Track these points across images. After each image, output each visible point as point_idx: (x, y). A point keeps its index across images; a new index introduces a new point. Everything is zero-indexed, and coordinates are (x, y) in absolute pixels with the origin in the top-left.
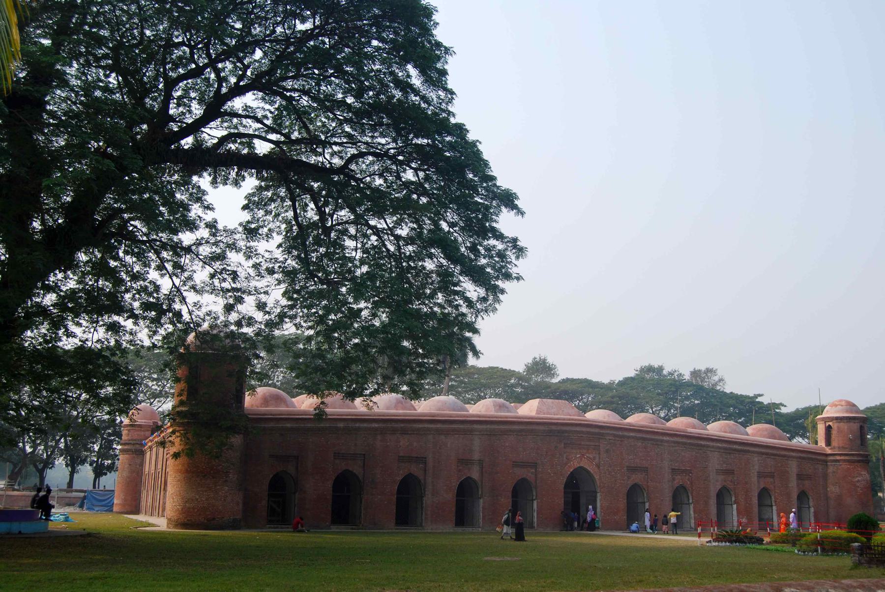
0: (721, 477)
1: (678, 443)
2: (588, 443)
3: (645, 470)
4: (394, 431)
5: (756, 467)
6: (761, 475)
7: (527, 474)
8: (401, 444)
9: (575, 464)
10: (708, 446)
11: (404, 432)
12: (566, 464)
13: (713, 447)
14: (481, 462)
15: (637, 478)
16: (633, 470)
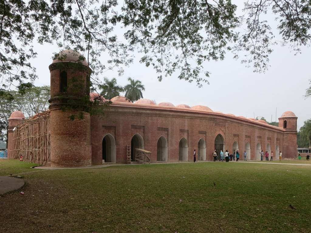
3: (238, 136)
4: (156, 115)
9: (218, 133)
11: (160, 115)
14: (188, 131)
16: (235, 135)
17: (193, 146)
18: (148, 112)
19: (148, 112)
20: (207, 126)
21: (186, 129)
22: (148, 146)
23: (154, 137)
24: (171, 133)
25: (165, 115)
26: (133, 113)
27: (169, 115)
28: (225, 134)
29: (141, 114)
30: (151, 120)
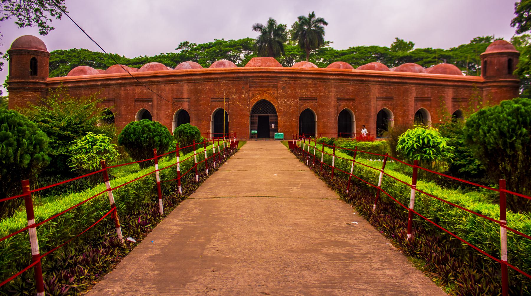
0: (380, 103)
1: (343, 80)
2: (268, 84)
4: (131, 84)
5: (414, 94)
6: (417, 100)
7: (224, 105)
8: (136, 91)
9: (259, 98)
10: (369, 81)
11: (138, 84)
12: (252, 98)
13: (374, 81)
15: (308, 105)
16: (304, 100)
17: (200, 120)
18: (120, 81)
19: (120, 81)
20: (229, 89)
21: (185, 96)
22: (120, 121)
23: (129, 110)
24: (157, 104)
25: (146, 82)
26: (97, 85)
27: (152, 82)
28: (277, 98)
29: (109, 85)
30: (124, 90)
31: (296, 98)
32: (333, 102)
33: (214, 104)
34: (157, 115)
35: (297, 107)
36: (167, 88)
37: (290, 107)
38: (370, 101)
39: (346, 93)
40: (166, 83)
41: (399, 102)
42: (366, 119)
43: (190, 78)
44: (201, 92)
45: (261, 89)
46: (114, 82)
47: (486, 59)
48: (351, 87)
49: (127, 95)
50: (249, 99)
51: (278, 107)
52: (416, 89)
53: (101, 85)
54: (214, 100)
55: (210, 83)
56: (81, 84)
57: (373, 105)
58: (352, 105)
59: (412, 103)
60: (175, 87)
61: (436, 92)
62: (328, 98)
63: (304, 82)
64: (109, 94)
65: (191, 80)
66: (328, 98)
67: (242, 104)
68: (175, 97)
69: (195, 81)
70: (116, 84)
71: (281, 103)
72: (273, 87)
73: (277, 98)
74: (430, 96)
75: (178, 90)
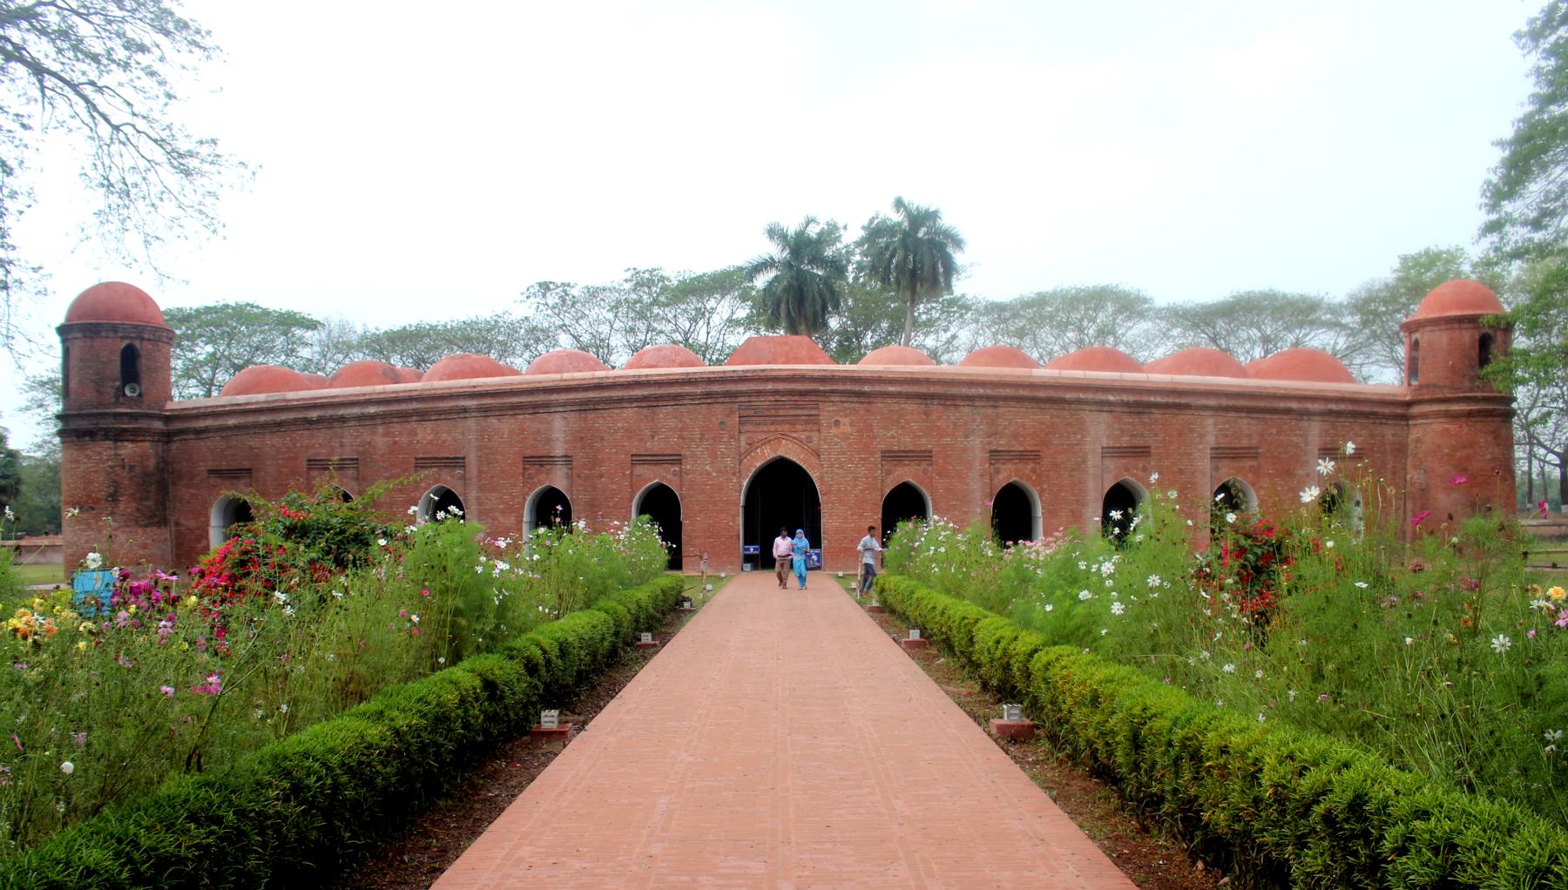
0: (1111, 464)
2: (792, 412)
3: (924, 456)
5: (1211, 440)
10: (1079, 402)
11: (423, 416)
12: (748, 452)
14: (568, 459)
16: (894, 457)
20: (682, 430)
21: (559, 450)
28: (817, 454)
29: (343, 419)
30: (385, 435)
31: (872, 454)
32: (977, 463)
33: (639, 470)
34: (480, 504)
35: (875, 478)
36: (506, 425)
37: (856, 479)
38: (1084, 462)
39: (1016, 436)
40: (501, 411)
41: (1167, 463)
42: (1073, 512)
43: (572, 396)
44: (602, 439)
45: (772, 428)
46: (356, 411)
47: (1417, 335)
48: (1030, 419)
49: (394, 447)
50: (741, 456)
51: (821, 478)
52: (1216, 424)
53: (320, 420)
54: (638, 459)
55: (630, 413)
56: (263, 418)
57: (1091, 471)
58: (1034, 471)
59: (1204, 464)
60: (528, 421)
61: (1274, 431)
62: (965, 450)
63: (896, 407)
64: (342, 445)
65: (574, 404)
66: (965, 450)
67: (719, 471)
68: (529, 453)
69: (585, 407)
70: (361, 418)
71: (831, 466)
72: (807, 423)
73: (817, 454)
74: (1254, 442)
75: (538, 432)
